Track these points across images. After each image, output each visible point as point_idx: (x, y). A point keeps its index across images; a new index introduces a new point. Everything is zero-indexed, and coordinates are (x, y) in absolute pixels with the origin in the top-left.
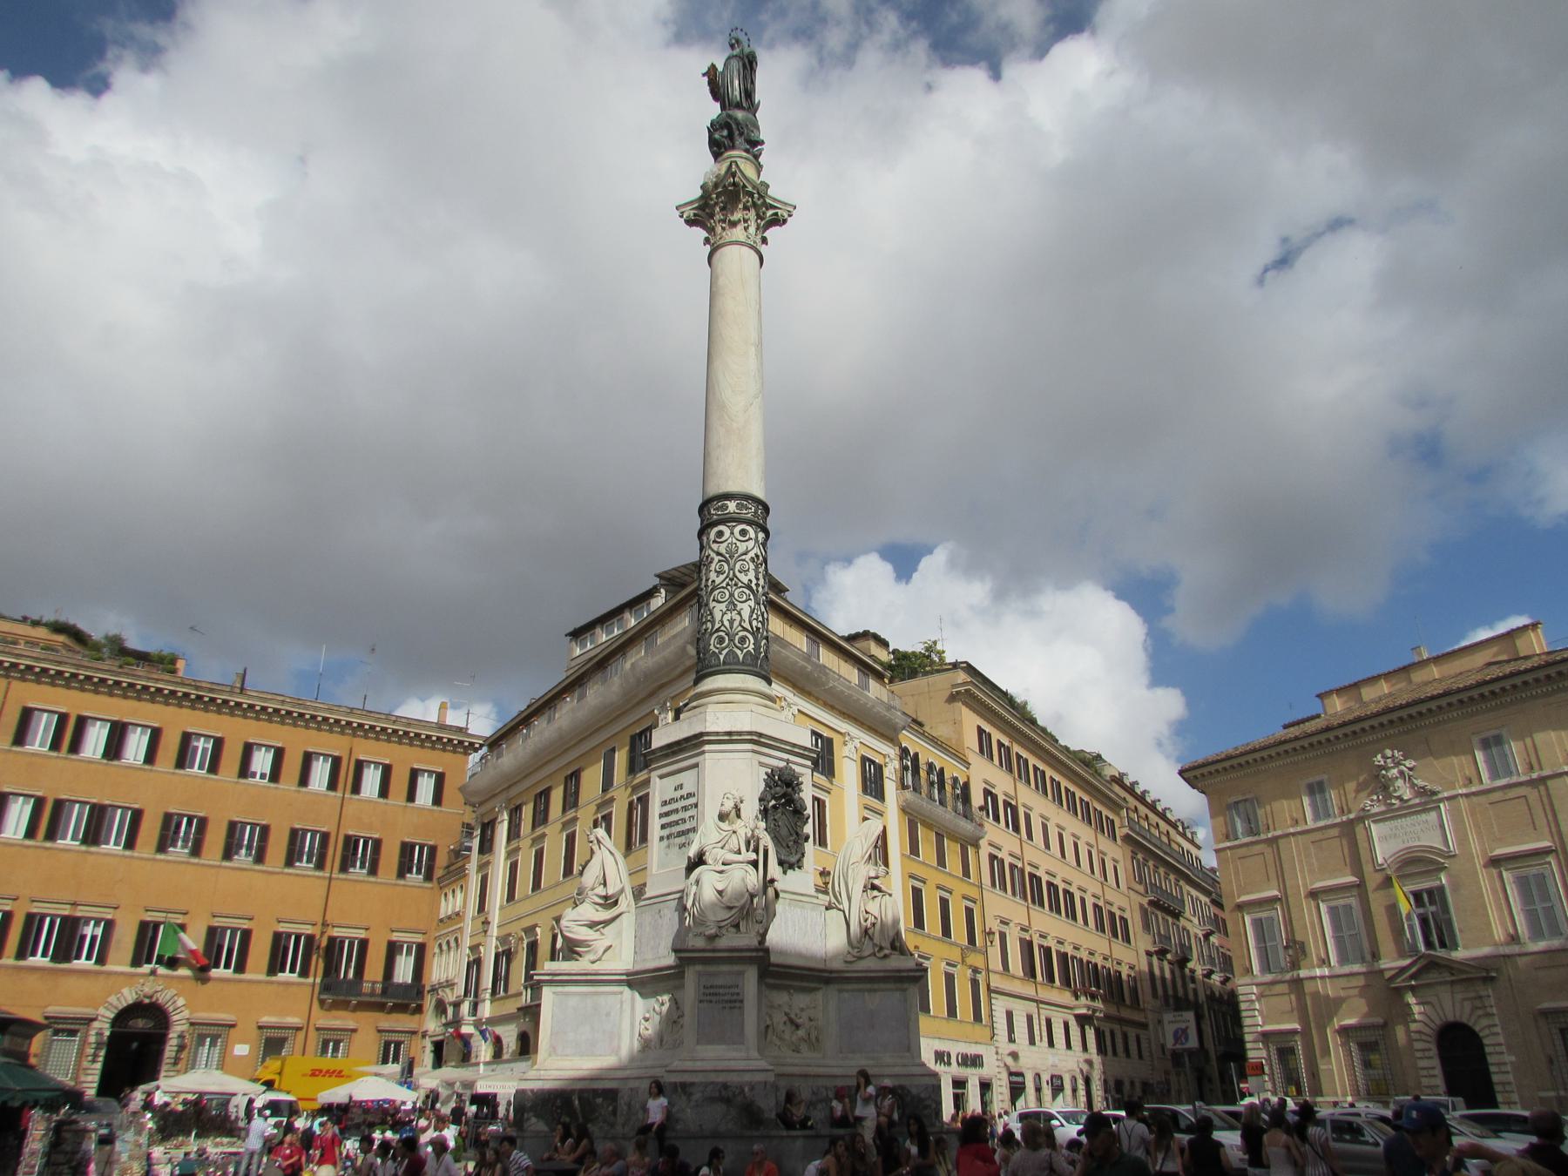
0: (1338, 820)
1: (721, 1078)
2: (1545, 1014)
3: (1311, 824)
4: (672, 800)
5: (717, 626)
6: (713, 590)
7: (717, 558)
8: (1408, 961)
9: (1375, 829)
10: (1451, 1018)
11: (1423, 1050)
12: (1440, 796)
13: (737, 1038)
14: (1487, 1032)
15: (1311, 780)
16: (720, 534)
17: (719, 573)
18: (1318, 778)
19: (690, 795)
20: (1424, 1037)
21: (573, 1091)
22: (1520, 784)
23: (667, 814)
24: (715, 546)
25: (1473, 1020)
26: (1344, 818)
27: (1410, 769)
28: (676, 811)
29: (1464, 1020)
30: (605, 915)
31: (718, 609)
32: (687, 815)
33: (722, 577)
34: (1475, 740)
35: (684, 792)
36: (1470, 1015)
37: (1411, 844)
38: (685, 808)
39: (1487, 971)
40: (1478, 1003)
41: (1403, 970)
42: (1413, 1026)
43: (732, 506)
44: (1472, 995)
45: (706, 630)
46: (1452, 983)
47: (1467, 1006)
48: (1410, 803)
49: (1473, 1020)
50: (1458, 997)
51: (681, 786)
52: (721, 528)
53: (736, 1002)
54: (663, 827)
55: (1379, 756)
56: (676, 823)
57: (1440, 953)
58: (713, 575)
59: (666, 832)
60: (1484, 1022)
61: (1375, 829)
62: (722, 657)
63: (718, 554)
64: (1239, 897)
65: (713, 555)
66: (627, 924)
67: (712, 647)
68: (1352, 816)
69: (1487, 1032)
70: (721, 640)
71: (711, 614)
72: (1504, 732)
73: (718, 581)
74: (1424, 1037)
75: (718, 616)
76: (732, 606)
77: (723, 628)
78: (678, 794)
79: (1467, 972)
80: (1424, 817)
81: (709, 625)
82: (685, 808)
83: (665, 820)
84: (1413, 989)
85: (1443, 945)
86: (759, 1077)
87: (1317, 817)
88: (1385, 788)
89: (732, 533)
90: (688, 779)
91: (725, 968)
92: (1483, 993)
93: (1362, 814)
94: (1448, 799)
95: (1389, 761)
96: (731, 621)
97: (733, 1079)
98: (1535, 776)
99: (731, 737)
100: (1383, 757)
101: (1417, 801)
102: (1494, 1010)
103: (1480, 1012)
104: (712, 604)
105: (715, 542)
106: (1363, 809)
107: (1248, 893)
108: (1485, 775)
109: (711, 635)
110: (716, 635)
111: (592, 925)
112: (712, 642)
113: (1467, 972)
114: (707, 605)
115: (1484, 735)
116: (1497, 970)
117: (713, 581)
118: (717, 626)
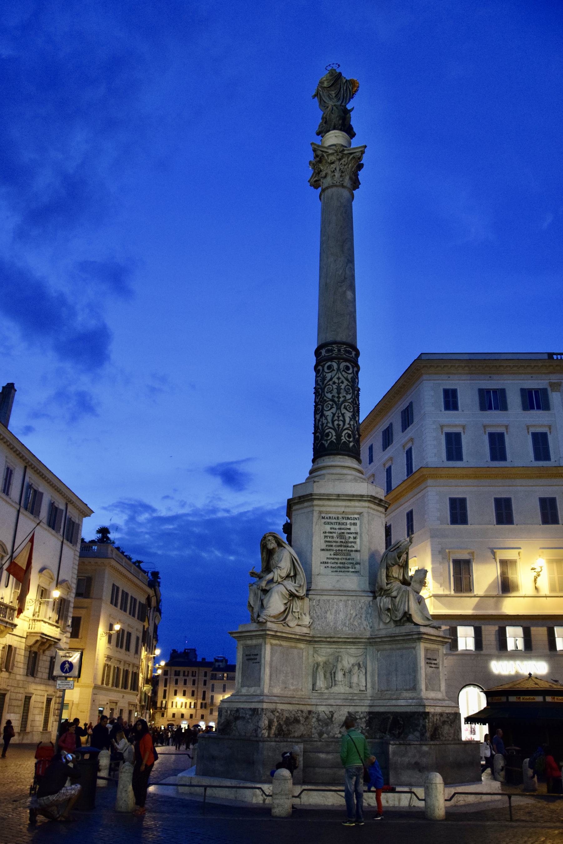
5: (347, 426)
7: (346, 382)
16: (347, 368)
17: (347, 393)
24: (343, 373)
33: (349, 397)
43: (354, 353)
45: (338, 425)
58: (342, 391)
63: (347, 380)
65: (343, 379)
67: (343, 438)
70: (349, 436)
71: (343, 415)
75: (347, 420)
77: (350, 429)
81: (341, 423)
89: (353, 371)
105: (343, 371)
110: (346, 431)
112: (343, 434)
114: (339, 408)
118: (347, 426)
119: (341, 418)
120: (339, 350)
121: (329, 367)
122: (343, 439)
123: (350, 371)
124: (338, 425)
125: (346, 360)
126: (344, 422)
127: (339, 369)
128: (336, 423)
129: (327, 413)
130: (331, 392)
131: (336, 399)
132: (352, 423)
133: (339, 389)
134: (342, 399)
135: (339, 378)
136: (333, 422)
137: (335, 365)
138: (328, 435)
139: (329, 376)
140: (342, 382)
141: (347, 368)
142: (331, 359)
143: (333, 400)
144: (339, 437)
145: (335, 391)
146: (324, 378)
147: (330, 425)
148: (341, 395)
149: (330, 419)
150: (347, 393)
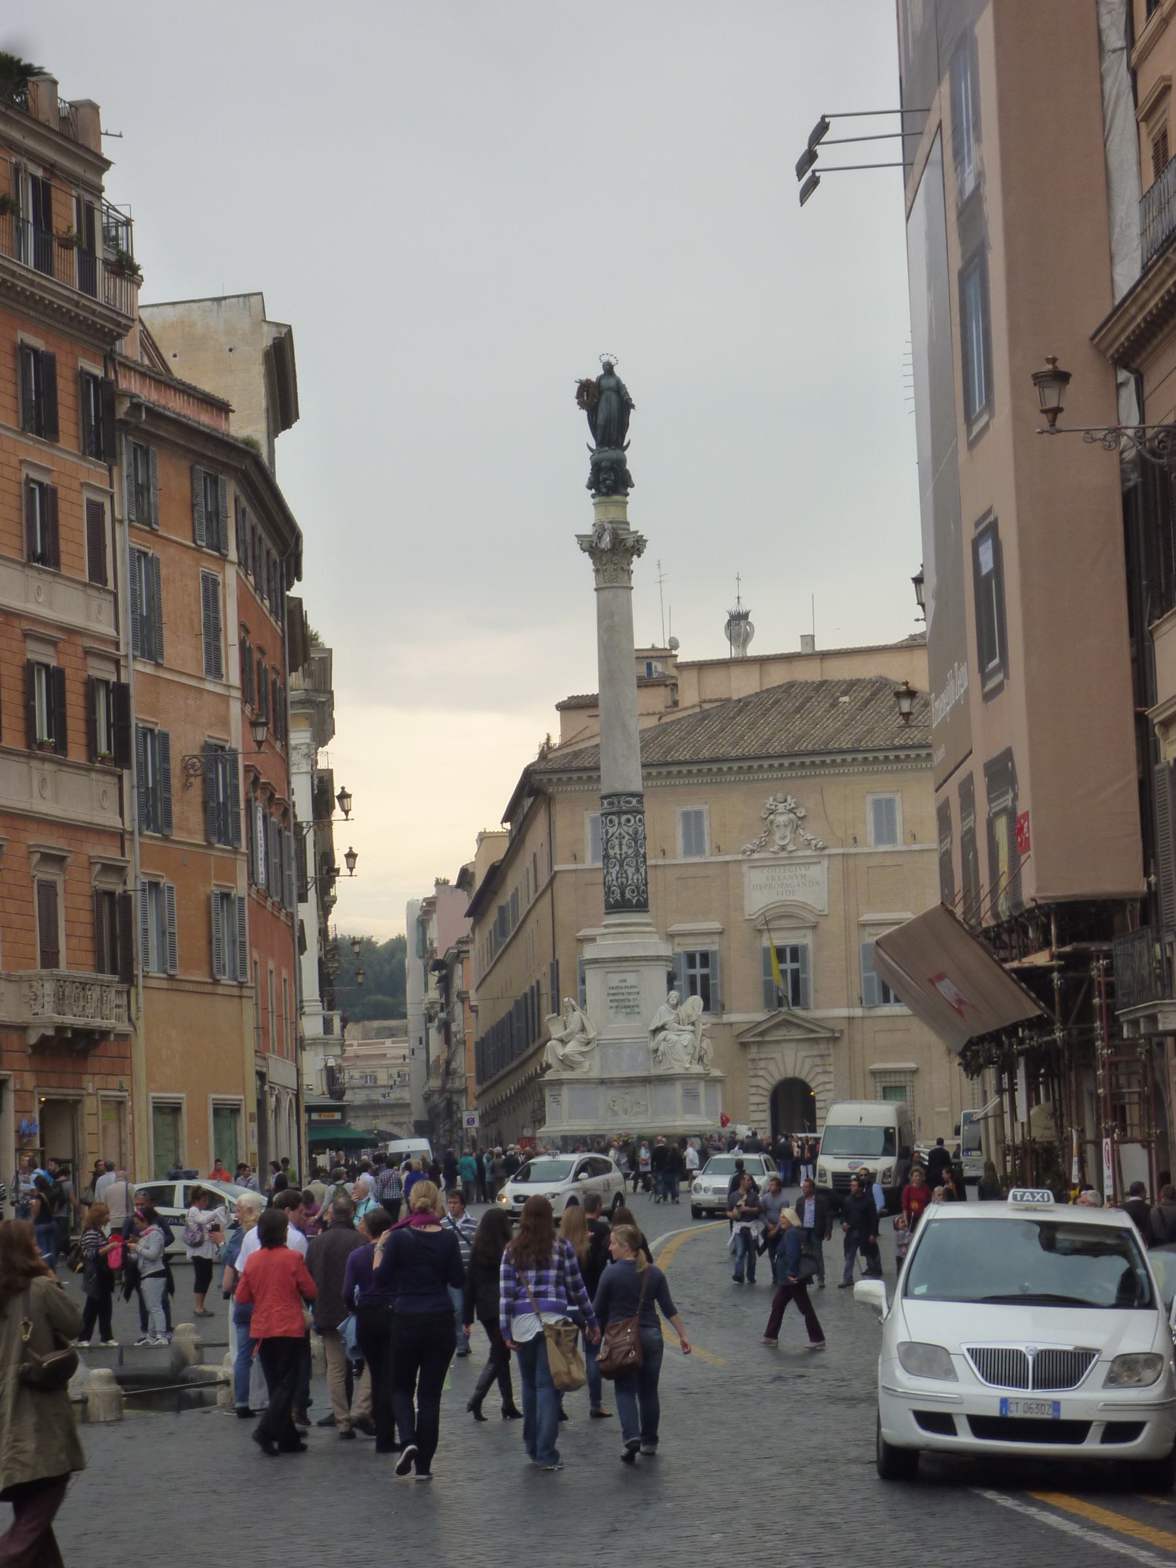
0: (713, 859)
1: (698, 1129)
2: (874, 1073)
3: (681, 860)
4: (617, 988)
5: (630, 882)
6: (625, 858)
7: (627, 837)
8: (760, 1016)
9: (754, 877)
10: (790, 1074)
11: (758, 1104)
12: (827, 852)
13: (695, 1111)
14: (820, 1088)
15: (689, 808)
16: (628, 821)
17: (629, 847)
18: (696, 808)
19: (632, 987)
20: (761, 1092)
21: (587, 1136)
22: (901, 852)
23: (614, 994)
25: (810, 1077)
26: (720, 859)
27: (800, 818)
28: (623, 994)
29: (802, 1077)
31: (631, 871)
32: (631, 997)
34: (870, 799)
35: (628, 984)
36: (809, 1072)
37: (785, 897)
38: (629, 994)
39: (833, 1031)
40: (818, 1061)
41: (759, 1024)
42: (755, 1081)
43: (634, 801)
44: (815, 1053)
46: (799, 1040)
47: (808, 1062)
48: (793, 854)
49: (810, 1077)
50: (802, 1054)
51: (625, 981)
52: (629, 816)
53: (696, 1096)
54: (611, 1001)
55: (771, 799)
56: (623, 1000)
57: (798, 1011)
58: (624, 847)
59: (615, 1004)
60: (821, 1079)
61: (754, 877)
62: (634, 902)
63: (628, 834)
64: (578, 931)
66: (596, 1051)
68: (728, 858)
69: (820, 1088)
70: (633, 892)
71: (626, 872)
72: (898, 797)
73: (630, 852)
74: (761, 1092)
75: (630, 877)
76: (638, 870)
78: (623, 984)
79: (813, 1031)
80: (803, 871)
81: (624, 880)
82: (629, 994)
84: (759, 1043)
85: (796, 1001)
86: (712, 1128)
87: (688, 852)
88: (770, 833)
90: (631, 979)
91: (692, 1081)
92: (826, 1052)
93: (740, 857)
94: (829, 855)
95: (781, 806)
96: (638, 879)
97: (703, 1129)
98: (916, 847)
99: (658, 958)
100: (775, 800)
101: (800, 853)
102: (831, 1069)
103: (819, 1069)
104: (626, 867)
106: (744, 853)
107: (591, 926)
108: (871, 838)
109: (626, 887)
111: (582, 1053)
112: (627, 891)
113: (813, 1031)
114: (621, 866)
115: (878, 797)
116: (842, 1032)
117: (626, 853)
118: (630, 882)
119: (624, 875)
120: (619, 802)
121: (611, 821)
122: (628, 896)
123: (632, 821)
124: (622, 883)
126: (627, 878)
127: (620, 823)
128: (619, 880)
129: (611, 870)
131: (618, 856)
132: (635, 877)
133: (621, 845)
134: (623, 856)
135: (620, 834)
136: (617, 879)
137: (616, 821)
138: (613, 893)
139: (611, 831)
140: (624, 837)
141: (628, 821)
143: (615, 858)
144: (623, 894)
145: (617, 847)
147: (615, 883)
148: (623, 852)
149: (614, 875)
150: (629, 847)
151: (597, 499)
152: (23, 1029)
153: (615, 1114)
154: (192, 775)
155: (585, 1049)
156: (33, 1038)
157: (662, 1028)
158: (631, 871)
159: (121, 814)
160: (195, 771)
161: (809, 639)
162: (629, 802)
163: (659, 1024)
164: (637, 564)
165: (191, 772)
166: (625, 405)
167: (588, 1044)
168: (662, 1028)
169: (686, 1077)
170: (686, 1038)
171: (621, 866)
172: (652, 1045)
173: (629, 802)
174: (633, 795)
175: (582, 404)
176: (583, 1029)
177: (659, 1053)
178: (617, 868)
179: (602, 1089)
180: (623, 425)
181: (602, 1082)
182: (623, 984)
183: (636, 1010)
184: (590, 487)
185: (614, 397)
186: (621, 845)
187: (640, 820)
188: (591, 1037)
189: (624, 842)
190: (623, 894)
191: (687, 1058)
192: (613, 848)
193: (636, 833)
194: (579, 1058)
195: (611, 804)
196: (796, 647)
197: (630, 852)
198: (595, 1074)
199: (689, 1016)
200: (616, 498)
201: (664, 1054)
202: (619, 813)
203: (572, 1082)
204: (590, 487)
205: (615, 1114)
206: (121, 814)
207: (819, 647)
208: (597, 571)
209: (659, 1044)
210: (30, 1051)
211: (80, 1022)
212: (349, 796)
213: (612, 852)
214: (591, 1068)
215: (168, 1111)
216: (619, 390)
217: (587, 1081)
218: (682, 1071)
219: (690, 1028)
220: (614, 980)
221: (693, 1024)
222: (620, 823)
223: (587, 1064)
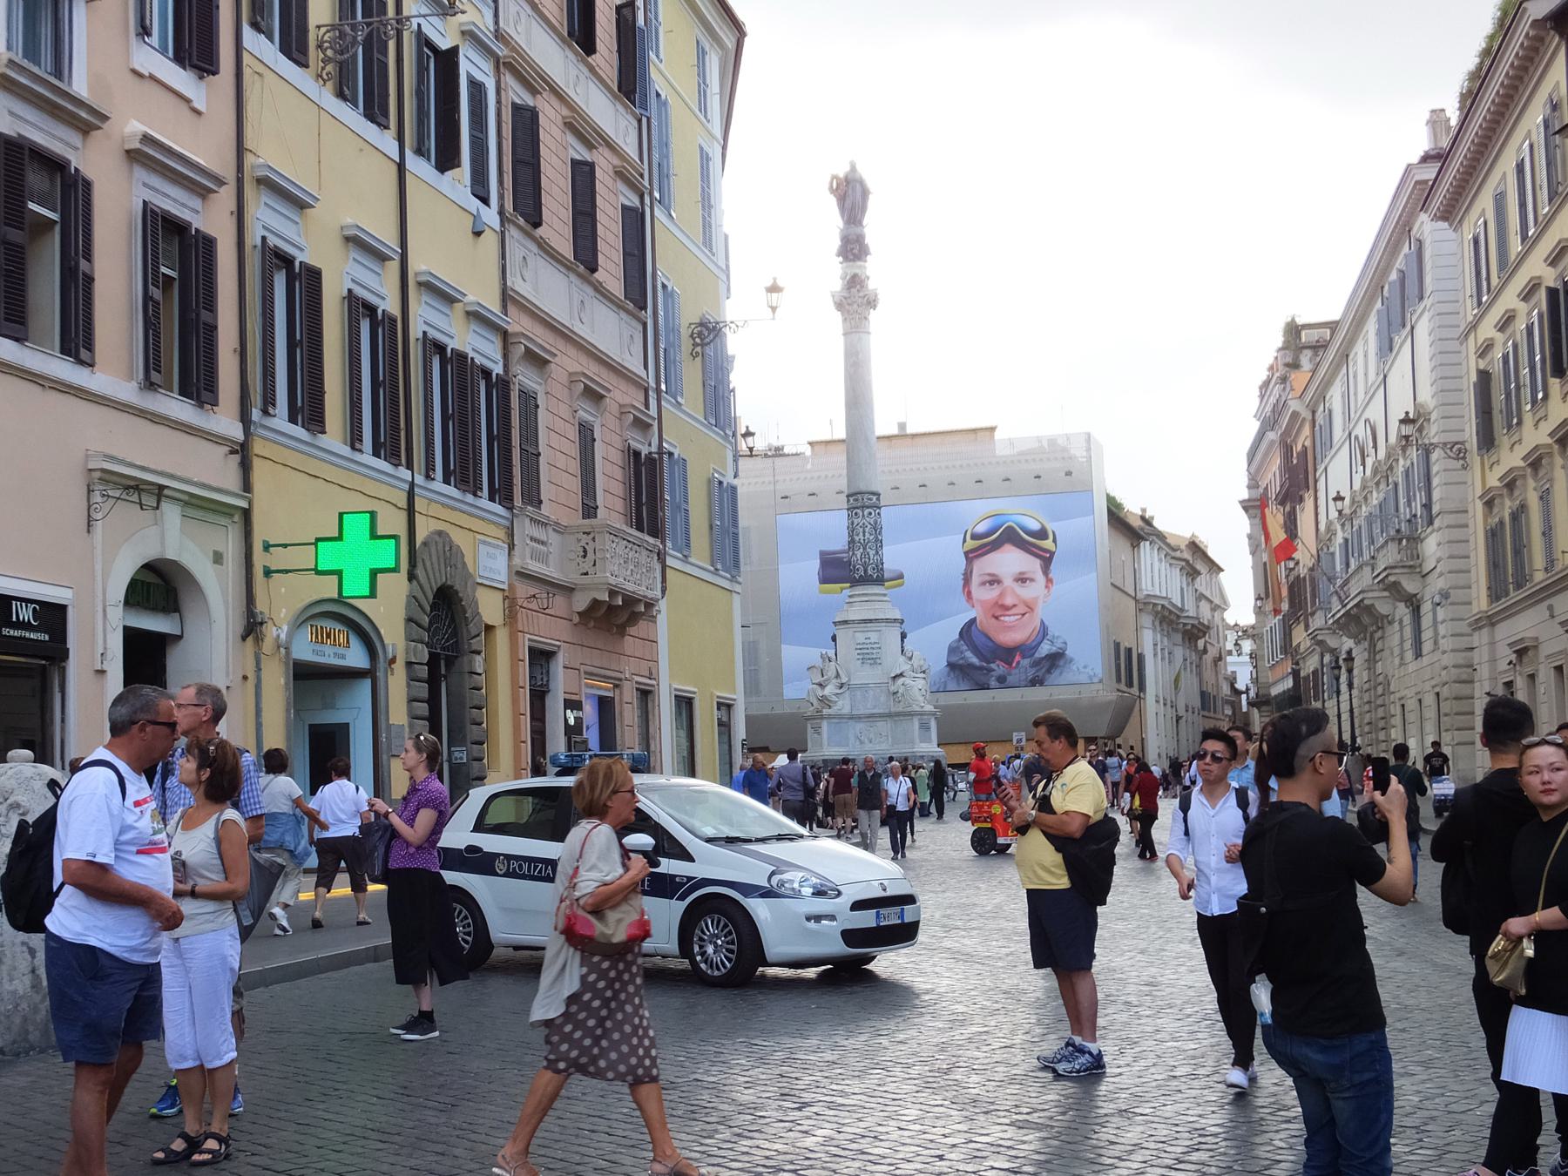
13: (930, 741)
16: (870, 514)
19: (875, 643)
30: (841, 691)
31: (872, 553)
32: (874, 651)
33: (871, 537)
35: (872, 640)
43: (875, 498)
58: (867, 535)
78: (868, 641)
83: (859, 651)
90: (874, 637)
114: (865, 549)
121: (856, 514)
122: (870, 572)
125: (868, 507)
127: (863, 516)
130: (858, 535)
133: (864, 532)
139: (856, 522)
141: (870, 514)
142: (857, 508)
144: (866, 571)
146: (853, 523)
151: (845, 264)
152: (568, 590)
153: (862, 742)
154: (698, 345)
155: (839, 691)
156: (581, 602)
157: (901, 675)
158: (872, 553)
159: (646, 367)
160: (702, 340)
161: (902, 426)
162: (870, 499)
163: (899, 672)
164: (874, 315)
165: (698, 340)
166: (865, 193)
167: (841, 688)
168: (901, 675)
169: (921, 714)
170: (920, 683)
171: (865, 549)
172: (893, 689)
173: (870, 499)
174: (874, 494)
175: (832, 190)
176: (838, 676)
177: (899, 695)
178: (861, 550)
179: (851, 722)
180: (864, 209)
181: (852, 717)
182: (868, 641)
183: (878, 661)
184: (838, 255)
185: (858, 185)
186: (864, 532)
187: (879, 514)
188: (844, 681)
189: (867, 530)
190: (866, 571)
191: (921, 699)
192: (858, 535)
193: (876, 523)
194: (834, 698)
195: (856, 500)
196: (895, 431)
197: (871, 537)
198: (846, 711)
199: (921, 667)
200: (859, 263)
201: (903, 695)
202: (863, 507)
203: (830, 717)
204: (838, 255)
205: (862, 742)
206: (646, 367)
207: (909, 431)
208: (845, 320)
209: (899, 687)
210: (576, 619)
211: (630, 587)
212: (752, 434)
213: (857, 538)
214: (843, 705)
215: (685, 704)
216: (862, 183)
217: (840, 717)
218: (918, 709)
219: (922, 675)
220: (861, 637)
221: (924, 672)
222: (863, 516)
223: (840, 703)
